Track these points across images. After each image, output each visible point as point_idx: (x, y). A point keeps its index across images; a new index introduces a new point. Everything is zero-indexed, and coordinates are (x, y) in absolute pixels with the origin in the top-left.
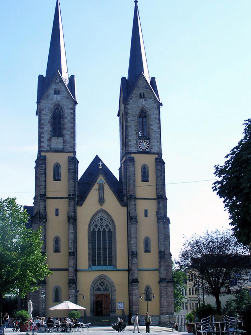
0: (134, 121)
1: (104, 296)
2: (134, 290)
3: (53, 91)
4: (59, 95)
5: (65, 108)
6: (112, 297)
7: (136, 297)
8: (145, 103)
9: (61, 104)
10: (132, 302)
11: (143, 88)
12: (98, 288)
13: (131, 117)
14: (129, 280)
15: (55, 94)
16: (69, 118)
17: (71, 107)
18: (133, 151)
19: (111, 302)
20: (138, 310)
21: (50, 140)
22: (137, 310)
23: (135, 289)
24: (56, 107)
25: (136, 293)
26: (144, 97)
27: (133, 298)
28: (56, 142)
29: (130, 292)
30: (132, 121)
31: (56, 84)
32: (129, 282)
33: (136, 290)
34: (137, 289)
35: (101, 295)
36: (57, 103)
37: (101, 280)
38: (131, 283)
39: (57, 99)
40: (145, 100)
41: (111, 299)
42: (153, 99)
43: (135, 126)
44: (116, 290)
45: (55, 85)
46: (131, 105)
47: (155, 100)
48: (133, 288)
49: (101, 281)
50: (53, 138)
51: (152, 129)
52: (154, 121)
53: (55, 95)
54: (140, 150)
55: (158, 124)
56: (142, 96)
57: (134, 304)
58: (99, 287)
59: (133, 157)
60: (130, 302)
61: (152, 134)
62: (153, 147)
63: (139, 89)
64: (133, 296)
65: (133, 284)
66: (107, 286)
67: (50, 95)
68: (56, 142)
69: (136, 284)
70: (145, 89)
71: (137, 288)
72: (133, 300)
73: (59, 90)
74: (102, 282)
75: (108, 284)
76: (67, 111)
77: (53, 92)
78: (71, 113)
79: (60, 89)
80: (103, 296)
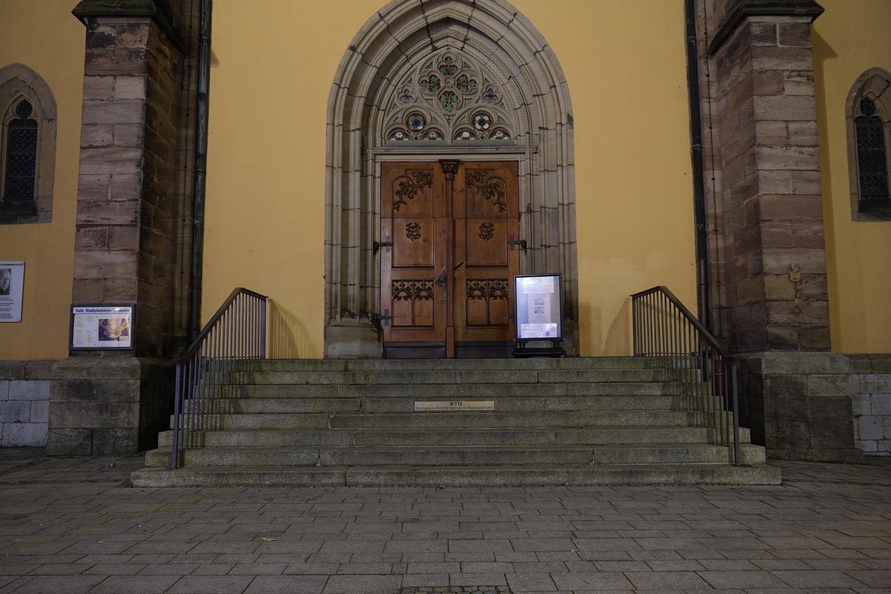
1: (468, 184)
2: (773, 88)
6: (531, 190)
7: (792, 152)
10: (757, 205)
12: (416, 118)
14: (691, 29)
19: (524, 233)
20: (824, 297)
22: (811, 289)
23: (778, 77)
25: (787, 122)
27: (762, 165)
29: (706, 131)
32: (700, 35)
33: (790, 89)
34: (800, 74)
35: (437, 170)
37: (435, 49)
38: (712, 51)
41: (529, 210)
44: (570, 119)
48: (756, 65)
49: (443, 51)
57: (768, 230)
58: (423, 107)
60: (710, 228)
64: (765, 151)
65: (756, 30)
66: (490, 95)
69: (783, 28)
71: (803, 66)
72: (765, 189)
74: (447, 68)
75: (498, 78)
80: (461, 172)
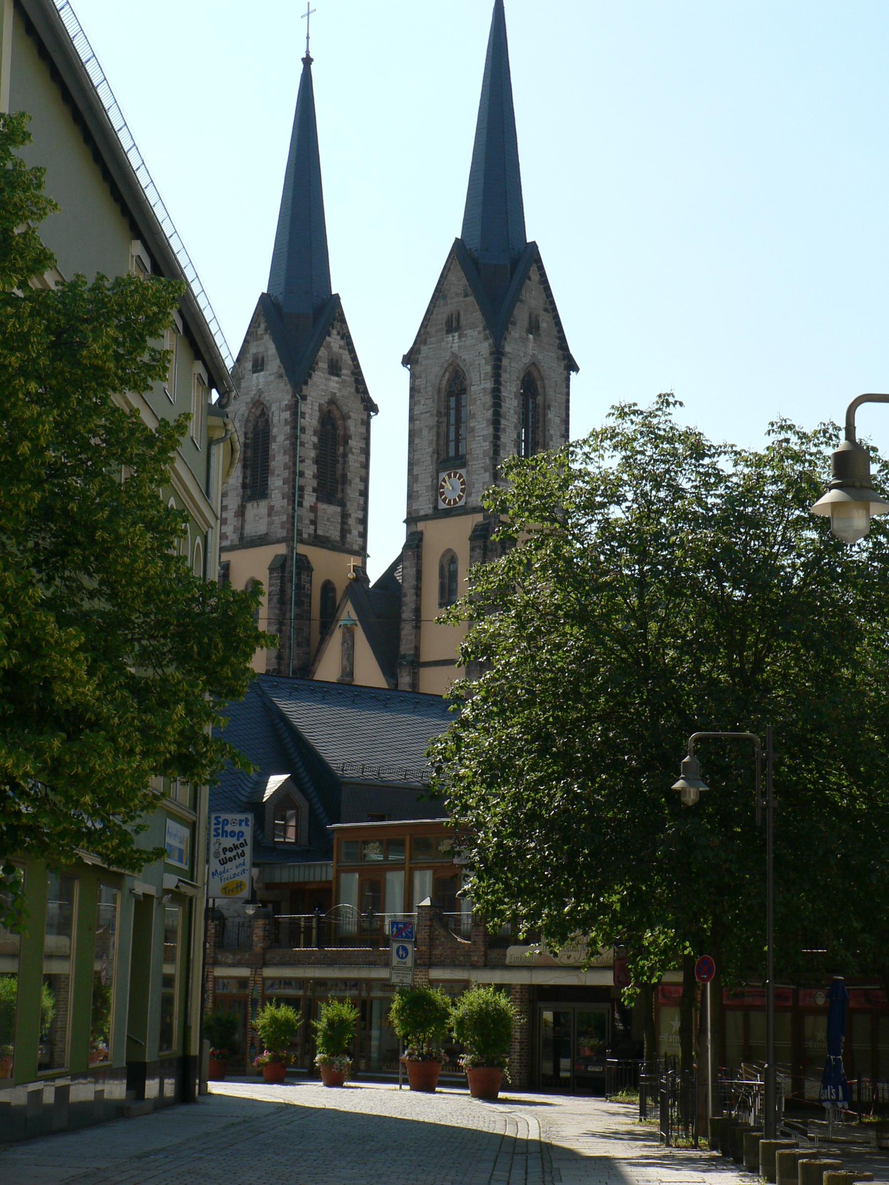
0: (428, 414)
3: (249, 365)
4: (262, 373)
5: (274, 408)
8: (459, 347)
9: (267, 397)
11: (457, 295)
13: (422, 402)
15: (254, 372)
16: (281, 438)
17: (286, 402)
18: (422, 513)
21: (241, 513)
24: (258, 413)
26: (458, 328)
28: (256, 515)
30: (424, 415)
31: (257, 340)
36: (257, 397)
39: (258, 385)
40: (460, 337)
42: (480, 328)
43: (430, 429)
45: (255, 343)
46: (424, 363)
47: (484, 329)
50: (249, 506)
51: (472, 430)
52: (478, 402)
53: (255, 375)
54: (442, 506)
55: (488, 410)
56: (454, 325)
59: (421, 533)
61: (472, 446)
62: (473, 490)
63: (446, 304)
67: (243, 378)
68: (256, 515)
70: (462, 299)
73: (263, 358)
76: (277, 418)
77: (250, 368)
78: (286, 420)
79: (265, 354)
